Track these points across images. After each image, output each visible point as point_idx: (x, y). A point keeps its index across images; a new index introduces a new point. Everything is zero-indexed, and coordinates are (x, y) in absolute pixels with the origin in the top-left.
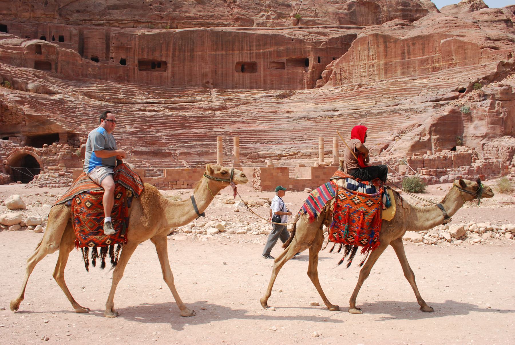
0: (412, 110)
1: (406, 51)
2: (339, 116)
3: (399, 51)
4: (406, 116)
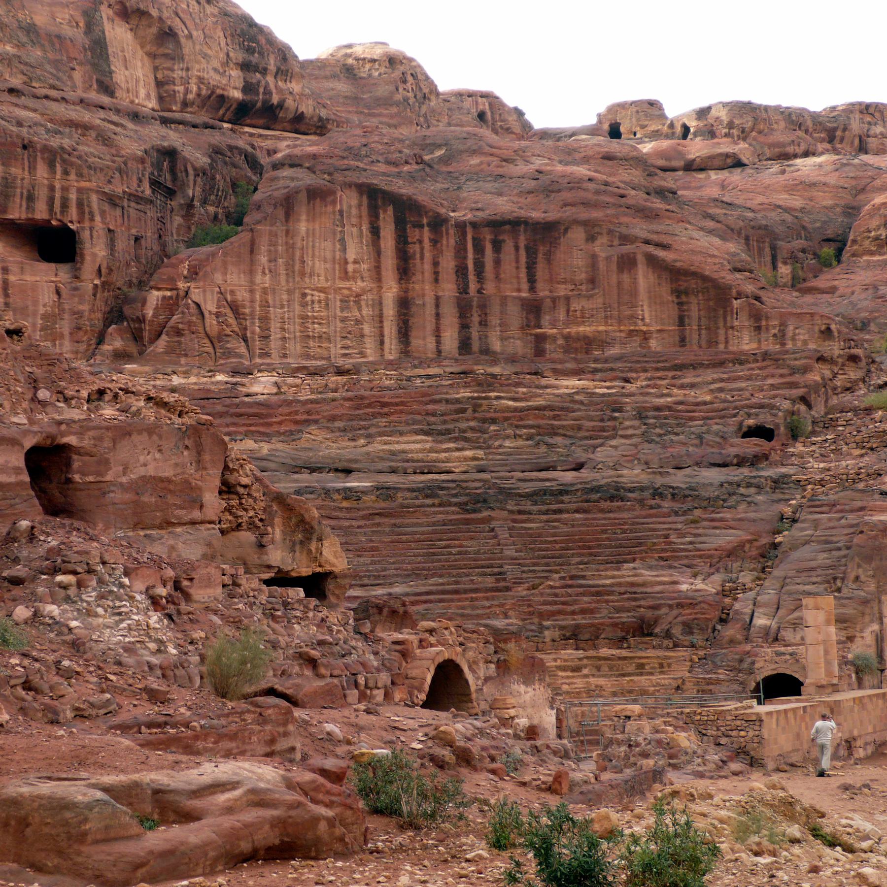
0: (676, 494)
3: (448, 263)
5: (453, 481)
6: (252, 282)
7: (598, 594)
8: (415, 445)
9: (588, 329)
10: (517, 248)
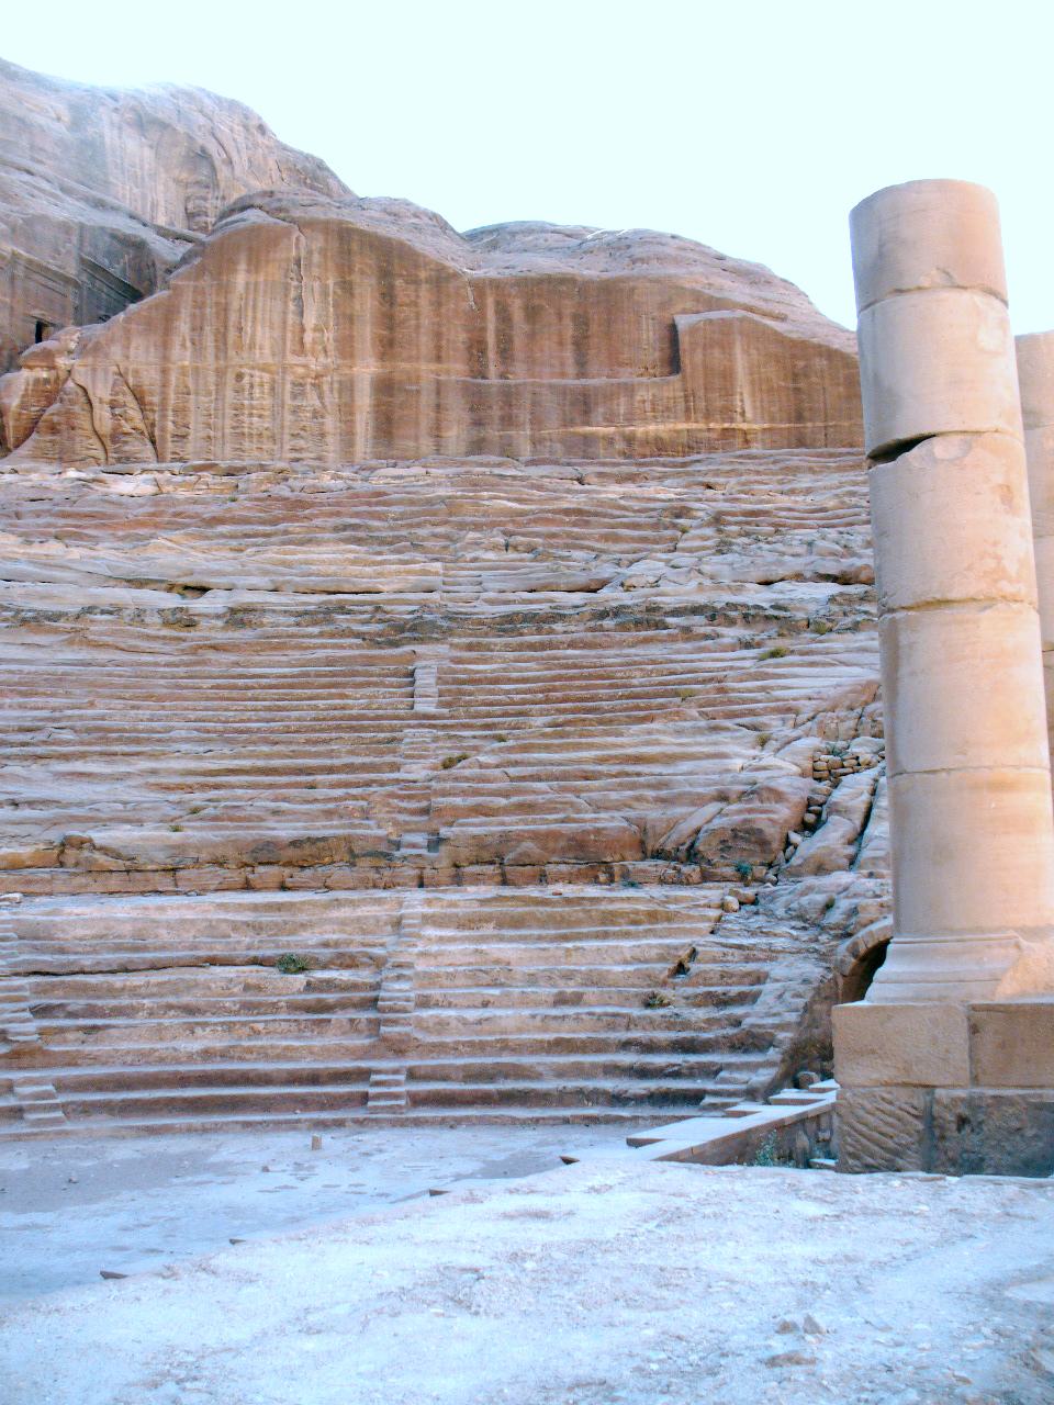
0: (750, 616)
1: (491, 339)
2: (238, 617)
3: (458, 336)
4: (748, 646)
5: (370, 603)
6: (165, 358)
7: (565, 777)
8: (330, 558)
9: (661, 427)
10: (560, 316)
